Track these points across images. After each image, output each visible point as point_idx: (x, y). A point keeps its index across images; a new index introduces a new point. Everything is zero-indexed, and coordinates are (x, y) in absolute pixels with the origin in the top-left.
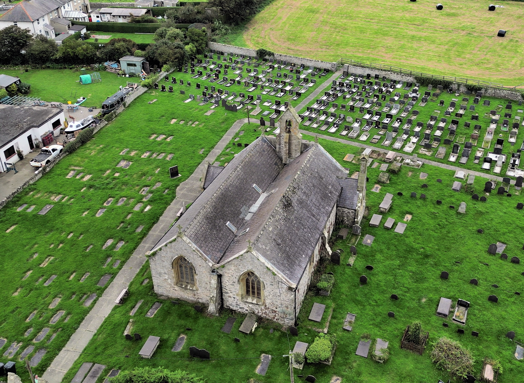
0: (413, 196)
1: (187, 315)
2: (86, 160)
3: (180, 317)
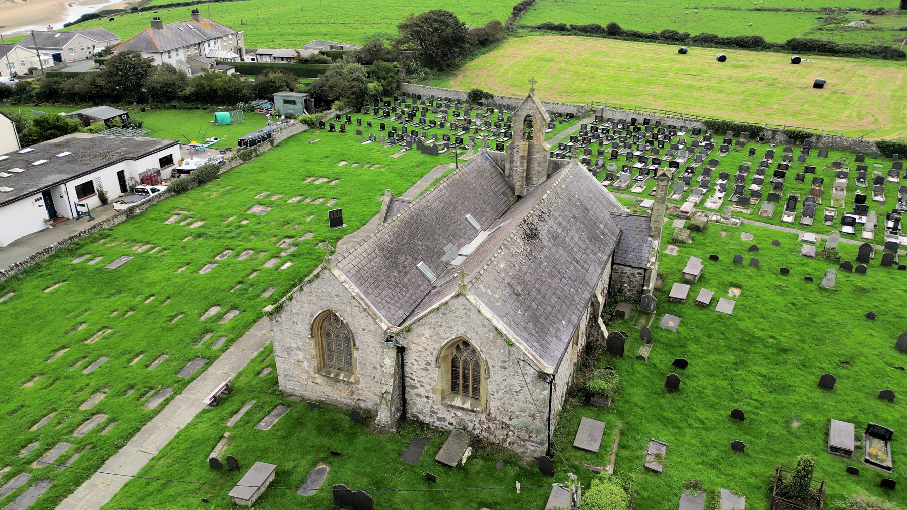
1: (335, 429)
2: (201, 204)
3: (320, 430)
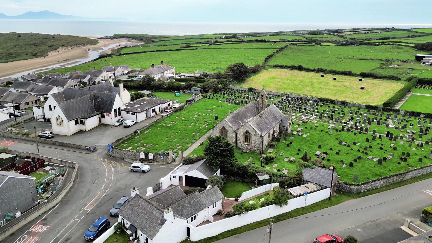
0: (311, 128)
